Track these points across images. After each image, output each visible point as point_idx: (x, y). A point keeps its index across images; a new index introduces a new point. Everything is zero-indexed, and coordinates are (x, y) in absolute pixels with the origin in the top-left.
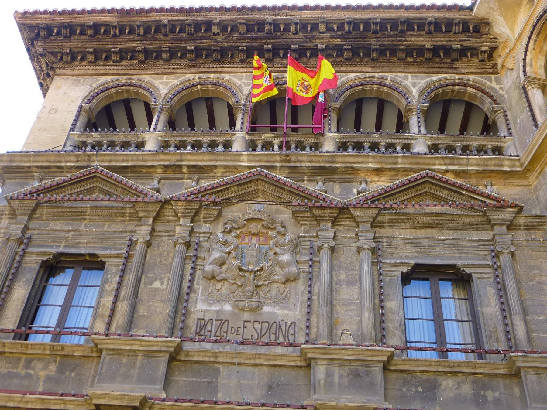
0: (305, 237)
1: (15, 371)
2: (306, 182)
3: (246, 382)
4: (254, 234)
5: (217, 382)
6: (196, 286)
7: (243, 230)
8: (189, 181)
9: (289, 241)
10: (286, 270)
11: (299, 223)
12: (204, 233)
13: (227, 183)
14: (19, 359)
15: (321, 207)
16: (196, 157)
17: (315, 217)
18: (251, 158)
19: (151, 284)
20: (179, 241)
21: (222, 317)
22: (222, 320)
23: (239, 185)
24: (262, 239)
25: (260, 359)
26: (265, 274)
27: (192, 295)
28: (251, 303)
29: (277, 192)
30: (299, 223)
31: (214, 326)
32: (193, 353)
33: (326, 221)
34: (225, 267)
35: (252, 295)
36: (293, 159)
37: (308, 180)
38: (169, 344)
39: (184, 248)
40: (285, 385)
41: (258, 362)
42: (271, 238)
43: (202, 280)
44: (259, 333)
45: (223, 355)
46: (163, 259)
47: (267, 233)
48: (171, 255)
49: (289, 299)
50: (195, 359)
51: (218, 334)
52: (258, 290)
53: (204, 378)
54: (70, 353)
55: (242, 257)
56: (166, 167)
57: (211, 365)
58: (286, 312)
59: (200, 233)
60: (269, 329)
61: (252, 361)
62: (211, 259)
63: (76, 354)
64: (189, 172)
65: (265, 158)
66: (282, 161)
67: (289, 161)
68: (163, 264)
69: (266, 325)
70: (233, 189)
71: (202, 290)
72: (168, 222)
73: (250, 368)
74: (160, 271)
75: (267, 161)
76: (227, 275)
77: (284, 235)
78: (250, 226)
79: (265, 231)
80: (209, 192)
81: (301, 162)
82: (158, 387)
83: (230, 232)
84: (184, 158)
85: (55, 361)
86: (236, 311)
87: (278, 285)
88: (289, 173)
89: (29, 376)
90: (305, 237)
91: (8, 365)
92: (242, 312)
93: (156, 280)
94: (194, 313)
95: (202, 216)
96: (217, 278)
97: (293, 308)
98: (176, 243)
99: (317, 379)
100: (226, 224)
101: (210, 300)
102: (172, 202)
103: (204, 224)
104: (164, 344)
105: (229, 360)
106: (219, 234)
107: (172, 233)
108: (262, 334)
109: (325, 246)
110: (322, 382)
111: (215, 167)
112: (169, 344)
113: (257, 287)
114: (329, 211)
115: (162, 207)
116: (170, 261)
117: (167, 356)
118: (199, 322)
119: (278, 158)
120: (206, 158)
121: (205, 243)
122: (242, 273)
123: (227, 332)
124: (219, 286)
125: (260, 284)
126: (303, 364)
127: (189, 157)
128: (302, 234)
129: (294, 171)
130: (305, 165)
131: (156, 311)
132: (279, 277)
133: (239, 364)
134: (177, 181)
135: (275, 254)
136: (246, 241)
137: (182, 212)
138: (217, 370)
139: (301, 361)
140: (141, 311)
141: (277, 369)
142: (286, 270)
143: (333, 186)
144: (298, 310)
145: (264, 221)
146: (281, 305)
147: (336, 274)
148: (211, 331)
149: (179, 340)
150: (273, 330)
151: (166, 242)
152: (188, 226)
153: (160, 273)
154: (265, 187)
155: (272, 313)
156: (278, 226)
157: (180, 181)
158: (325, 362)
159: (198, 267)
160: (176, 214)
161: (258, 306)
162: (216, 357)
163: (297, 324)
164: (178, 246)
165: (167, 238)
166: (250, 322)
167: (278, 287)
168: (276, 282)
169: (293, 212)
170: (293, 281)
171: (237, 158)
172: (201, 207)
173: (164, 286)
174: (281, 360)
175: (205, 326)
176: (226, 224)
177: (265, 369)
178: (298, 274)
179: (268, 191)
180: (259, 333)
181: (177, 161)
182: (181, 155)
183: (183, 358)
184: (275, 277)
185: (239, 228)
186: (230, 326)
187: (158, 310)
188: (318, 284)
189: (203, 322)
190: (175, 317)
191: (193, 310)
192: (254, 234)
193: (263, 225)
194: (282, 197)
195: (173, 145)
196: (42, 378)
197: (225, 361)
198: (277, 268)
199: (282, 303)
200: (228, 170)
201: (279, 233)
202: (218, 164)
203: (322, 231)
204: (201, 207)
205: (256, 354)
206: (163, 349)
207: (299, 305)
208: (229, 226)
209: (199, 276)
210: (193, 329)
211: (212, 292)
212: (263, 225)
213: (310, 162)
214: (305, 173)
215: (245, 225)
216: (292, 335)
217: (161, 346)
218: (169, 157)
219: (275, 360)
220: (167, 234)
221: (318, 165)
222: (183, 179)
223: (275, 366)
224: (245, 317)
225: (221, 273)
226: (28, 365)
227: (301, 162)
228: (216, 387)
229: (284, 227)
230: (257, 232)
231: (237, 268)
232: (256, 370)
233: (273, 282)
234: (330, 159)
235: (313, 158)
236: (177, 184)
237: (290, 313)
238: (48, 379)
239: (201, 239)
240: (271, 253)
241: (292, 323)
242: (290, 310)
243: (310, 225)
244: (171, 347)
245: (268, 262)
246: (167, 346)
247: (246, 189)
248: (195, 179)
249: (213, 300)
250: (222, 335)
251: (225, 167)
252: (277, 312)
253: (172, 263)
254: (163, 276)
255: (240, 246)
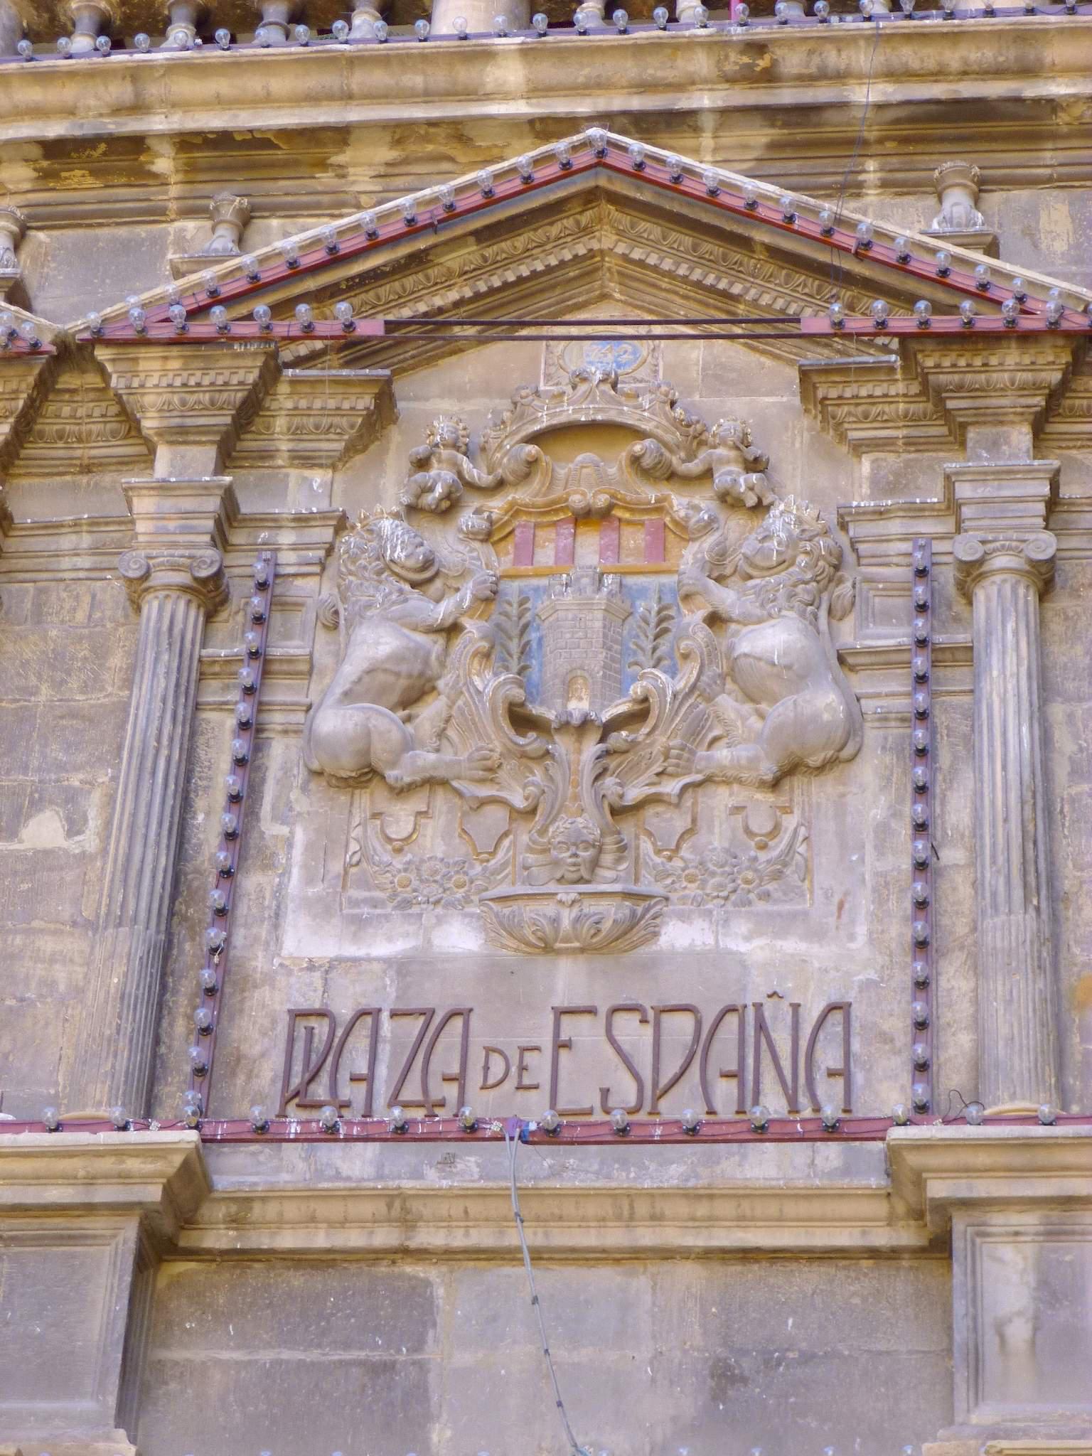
0: (881, 514)
2: (872, 196)
3: (584, 1354)
4: (586, 517)
5: (422, 1367)
6: (270, 827)
7: (521, 495)
8: (190, 225)
9: (792, 542)
10: (781, 711)
11: (842, 437)
12: (302, 521)
13: (413, 229)
15: (969, 338)
16: (221, 86)
17: (933, 393)
18: (549, 72)
19: (12, 833)
20: (159, 578)
21: (436, 997)
22: (428, 1014)
23: (486, 235)
24: (634, 539)
25: (656, 1218)
26: (661, 740)
27: (253, 882)
28: (590, 907)
29: (711, 263)
30: (842, 437)
31: (385, 1051)
32: (272, 1210)
33: (997, 419)
34: (430, 712)
35: (595, 864)
36: (792, 61)
37: (885, 184)
38: (133, 1165)
39: (187, 615)
40: (807, 1358)
41: (647, 1237)
42: (685, 532)
43: (304, 789)
44: (647, 1075)
45: (443, 1208)
46: (74, 684)
47: (660, 508)
48: (117, 660)
49: (807, 871)
50: (288, 1240)
51: (411, 1091)
52: (628, 828)
53: (347, 1346)
55: (524, 650)
56: (55, 149)
57: (383, 1269)
58: (792, 945)
59: (275, 523)
60: (702, 1045)
61: (615, 1237)
62: (351, 670)
64: (191, 171)
65: (630, 69)
66: (731, 80)
67: (770, 77)
68: (73, 715)
69: (681, 1026)
70: (454, 260)
71: (309, 847)
72: (87, 469)
73: (605, 1277)
74: (56, 752)
75: (644, 87)
76: (448, 755)
77: (760, 508)
78: (562, 472)
79: (651, 493)
80: (311, 284)
81: (841, 77)
82: (86, 1405)
83: (448, 508)
84: (153, 90)
86: (507, 955)
87: (739, 795)
88: (773, 146)
90: (881, 514)
92: (542, 961)
93: (37, 805)
94: (269, 979)
95: (280, 423)
96: (391, 774)
97: (832, 920)
98: (138, 588)
99: (988, 1319)
100: (422, 464)
101: (355, 903)
102: (102, 354)
103: (294, 473)
104: (107, 1164)
105: (482, 1237)
106: (387, 525)
107: (112, 534)
108: (664, 1080)
109: (1000, 561)
110: (1019, 1332)
111: (342, 134)
112: (133, 1165)
113: (618, 812)
114: (1012, 356)
115: (44, 387)
116: (112, 691)
117: (129, 1232)
118: (301, 1033)
119: (702, 64)
120: (280, 84)
121: (311, 583)
122: (530, 741)
123: (460, 1079)
124: (401, 817)
125: (634, 793)
126: (907, 1236)
127: (185, 87)
128: (862, 499)
129: (801, 134)
130: (865, 94)
131: (51, 985)
132: (744, 752)
133: (539, 1255)
134: (123, 232)
135: (715, 620)
136: (546, 556)
137: (165, 409)
138: (419, 1298)
139: (891, 1220)
141: (756, 1270)
142: (781, 711)
143: (1032, 212)
144: (862, 930)
145: (639, 434)
146: (761, 906)
147: (1070, 717)
148: (369, 1079)
149: (193, 1136)
150: (725, 1052)
151: (81, 588)
152: (206, 489)
153: (61, 767)
154: (637, 241)
155: (714, 959)
156: (723, 461)
157: (142, 231)
158: (1030, 1220)
159: (276, 719)
160: (128, 421)
161: (634, 921)
162: (408, 1222)
163: (856, 1012)
164: (151, 606)
165: (85, 562)
166: (591, 1011)
167: (737, 809)
168: (727, 782)
169: (805, 374)
170: (821, 769)
171: (464, 74)
172: (271, 372)
173: (89, 840)
174: (780, 1220)
175: (336, 1048)
176: (422, 464)
177: (689, 1273)
178: (853, 726)
179: (652, 260)
180: (647, 1075)
181: (117, 111)
182: (135, 74)
183: (217, 1238)
184: (722, 754)
185: (500, 484)
186: (477, 1044)
187: (60, 974)
188: (967, 779)
189: (321, 1028)
190: (160, 1009)
191: (259, 962)
192: (586, 517)
193: (635, 460)
194: (737, 289)
195: (86, 21)
197: (459, 1240)
198: (728, 704)
199: (766, 896)
200: (414, 148)
201: (729, 500)
202: (354, 114)
203: (983, 476)
204: (271, 372)
205: (631, 1196)
206: (104, 1194)
207: (864, 902)
208: (440, 477)
209: (286, 771)
210: (268, 1072)
211: (365, 855)
212: (635, 460)
213: (893, 75)
214: (865, 143)
215: (532, 463)
216: (832, 1074)
217: (91, 1180)
218: (67, 93)
219: (742, 1220)
220: (86, 540)
221: (938, 91)
222: (157, 214)
223: (747, 1255)
224: (560, 985)
225: (408, 744)
227: (841, 77)
228: (419, 1393)
229: (755, 465)
230: (602, 501)
231: (501, 711)
232: (640, 1283)
233: (708, 780)
234: (1009, 55)
235: (909, 55)
236: (127, 246)
237: (819, 954)
239: (288, 558)
240: (693, 618)
241: (832, 1008)
242: (817, 934)
243: (910, 442)
244: (146, 1179)
245: (673, 672)
246: (124, 1178)
247: (527, 254)
248: (228, 212)
249: (375, 904)
250: (435, 1095)
251: (400, 132)
252: (743, 947)
253: (125, 707)
254: (75, 780)
255: (512, 589)
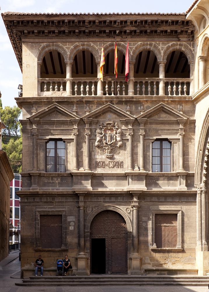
1: (49, 181)
14: (49, 177)
41: (114, 175)
50: (97, 175)
54: (63, 175)
60: (116, 164)
63: (65, 175)
69: (115, 163)
85: (59, 178)
89: (53, 183)
91: (47, 180)
140: (80, 159)
177: (115, 177)
196: (57, 183)
226: (52, 180)
237: (121, 158)
238: (59, 183)
